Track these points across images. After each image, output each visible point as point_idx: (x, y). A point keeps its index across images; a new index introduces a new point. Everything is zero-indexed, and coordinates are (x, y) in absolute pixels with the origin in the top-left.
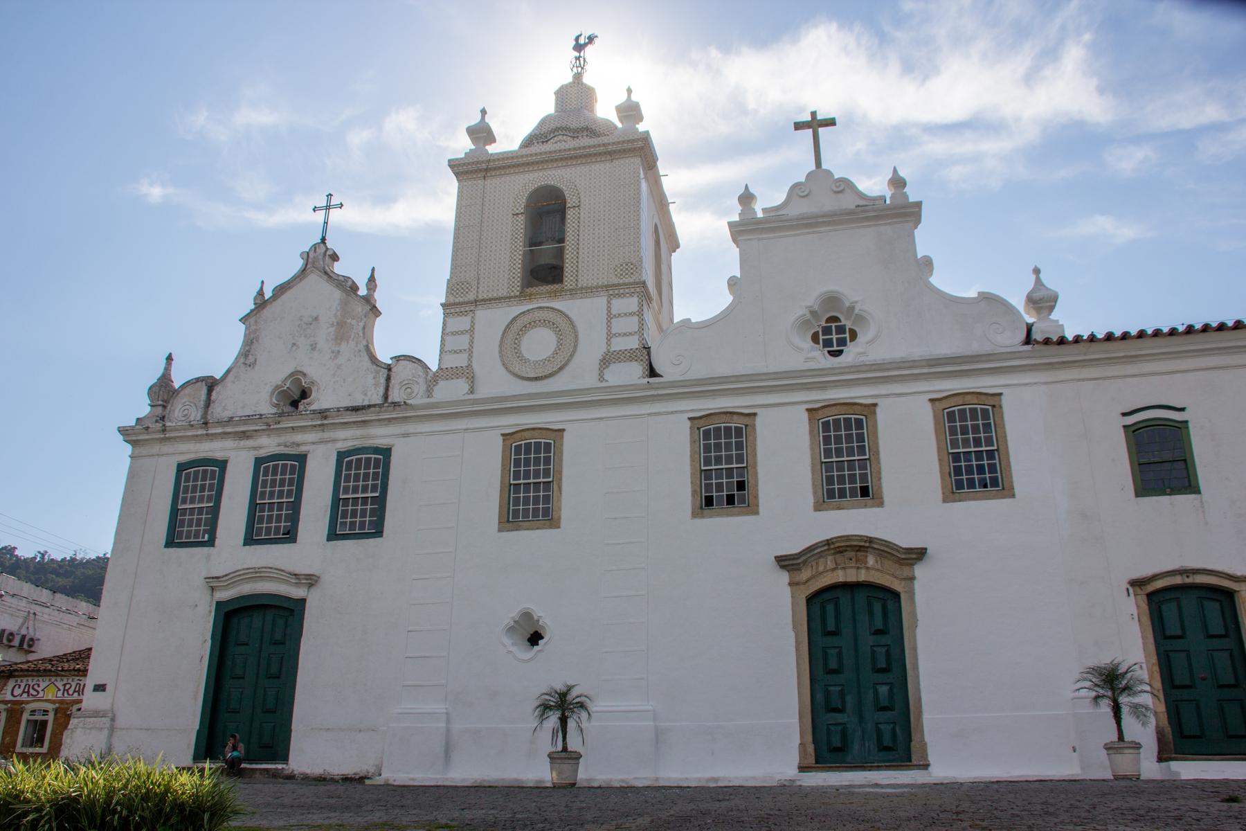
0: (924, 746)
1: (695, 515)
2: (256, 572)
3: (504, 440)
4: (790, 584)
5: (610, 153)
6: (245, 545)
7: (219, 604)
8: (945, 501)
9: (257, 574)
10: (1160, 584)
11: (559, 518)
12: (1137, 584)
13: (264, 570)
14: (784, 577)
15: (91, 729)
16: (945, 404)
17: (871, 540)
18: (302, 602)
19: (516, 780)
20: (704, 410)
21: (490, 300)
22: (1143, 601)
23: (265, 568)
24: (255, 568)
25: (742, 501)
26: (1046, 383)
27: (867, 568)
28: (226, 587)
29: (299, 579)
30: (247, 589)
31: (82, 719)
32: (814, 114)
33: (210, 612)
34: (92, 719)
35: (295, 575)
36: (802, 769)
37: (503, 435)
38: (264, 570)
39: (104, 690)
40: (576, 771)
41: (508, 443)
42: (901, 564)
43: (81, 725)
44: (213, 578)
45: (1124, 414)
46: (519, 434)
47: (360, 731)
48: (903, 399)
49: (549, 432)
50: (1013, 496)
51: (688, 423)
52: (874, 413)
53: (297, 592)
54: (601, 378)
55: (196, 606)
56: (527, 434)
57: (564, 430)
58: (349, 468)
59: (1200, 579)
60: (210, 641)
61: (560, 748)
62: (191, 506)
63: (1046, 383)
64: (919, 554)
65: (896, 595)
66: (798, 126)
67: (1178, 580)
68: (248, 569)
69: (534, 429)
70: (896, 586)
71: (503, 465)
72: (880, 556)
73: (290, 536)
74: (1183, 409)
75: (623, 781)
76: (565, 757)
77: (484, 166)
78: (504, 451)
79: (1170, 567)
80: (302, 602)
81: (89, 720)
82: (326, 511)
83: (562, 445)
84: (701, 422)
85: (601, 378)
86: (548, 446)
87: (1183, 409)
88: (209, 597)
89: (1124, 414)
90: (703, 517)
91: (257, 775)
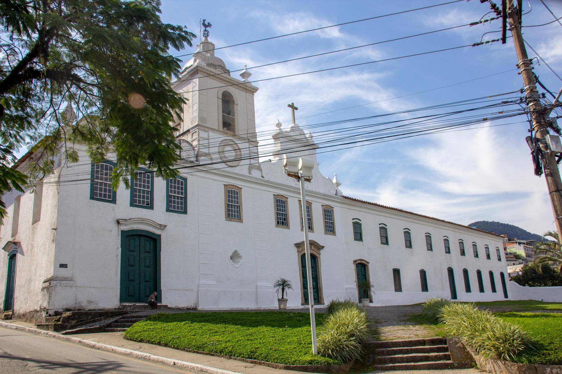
0: (324, 298)
1: (276, 226)
2: (142, 220)
3: (225, 187)
4: (298, 252)
5: (246, 89)
6: (115, 203)
7: (122, 231)
8: (325, 234)
9: (142, 221)
10: (358, 262)
11: (242, 220)
12: (355, 261)
13: (146, 220)
14: (296, 249)
15: (65, 286)
16: (324, 207)
17: (315, 242)
18: (160, 236)
19: (241, 308)
20: (276, 193)
21: (214, 129)
22: (355, 265)
23: (147, 219)
24: (142, 219)
25: (285, 224)
26: (341, 207)
27: (312, 250)
28: (126, 225)
29: (161, 226)
30: (135, 227)
31: (58, 281)
32: (293, 104)
33: (119, 235)
34: (65, 282)
35: (160, 225)
36: (302, 304)
37: (224, 185)
38: (146, 220)
39: (67, 267)
40: (286, 305)
41: (226, 188)
42: (318, 249)
43: (58, 284)
44: (123, 220)
45: (353, 219)
46: (229, 186)
47: (187, 290)
48: (316, 203)
49: (238, 188)
50: (336, 235)
51: (273, 196)
52: (311, 205)
53: (158, 232)
54: (250, 173)
55: (111, 231)
56: (232, 187)
57: (242, 188)
58: (171, 182)
59: (363, 262)
60: (120, 249)
61: (280, 297)
62: (101, 181)
63: (341, 207)
64: (323, 247)
65: (317, 257)
66: (289, 106)
67: (360, 262)
68: (139, 218)
69: (233, 185)
70: (317, 255)
71: (225, 196)
72: (314, 247)
73: (150, 206)
74: (360, 221)
75: (268, 308)
76: (282, 300)
77: (209, 72)
78: (225, 191)
79: (359, 259)
80: (160, 236)
81: (63, 282)
82: (164, 198)
83: (241, 194)
84: (276, 196)
85: (250, 173)
86: (237, 192)
87: (360, 221)
88: (117, 228)
89: (353, 219)
90: (278, 227)
91: (162, 308)
